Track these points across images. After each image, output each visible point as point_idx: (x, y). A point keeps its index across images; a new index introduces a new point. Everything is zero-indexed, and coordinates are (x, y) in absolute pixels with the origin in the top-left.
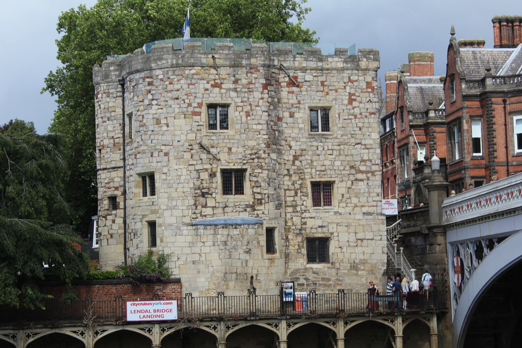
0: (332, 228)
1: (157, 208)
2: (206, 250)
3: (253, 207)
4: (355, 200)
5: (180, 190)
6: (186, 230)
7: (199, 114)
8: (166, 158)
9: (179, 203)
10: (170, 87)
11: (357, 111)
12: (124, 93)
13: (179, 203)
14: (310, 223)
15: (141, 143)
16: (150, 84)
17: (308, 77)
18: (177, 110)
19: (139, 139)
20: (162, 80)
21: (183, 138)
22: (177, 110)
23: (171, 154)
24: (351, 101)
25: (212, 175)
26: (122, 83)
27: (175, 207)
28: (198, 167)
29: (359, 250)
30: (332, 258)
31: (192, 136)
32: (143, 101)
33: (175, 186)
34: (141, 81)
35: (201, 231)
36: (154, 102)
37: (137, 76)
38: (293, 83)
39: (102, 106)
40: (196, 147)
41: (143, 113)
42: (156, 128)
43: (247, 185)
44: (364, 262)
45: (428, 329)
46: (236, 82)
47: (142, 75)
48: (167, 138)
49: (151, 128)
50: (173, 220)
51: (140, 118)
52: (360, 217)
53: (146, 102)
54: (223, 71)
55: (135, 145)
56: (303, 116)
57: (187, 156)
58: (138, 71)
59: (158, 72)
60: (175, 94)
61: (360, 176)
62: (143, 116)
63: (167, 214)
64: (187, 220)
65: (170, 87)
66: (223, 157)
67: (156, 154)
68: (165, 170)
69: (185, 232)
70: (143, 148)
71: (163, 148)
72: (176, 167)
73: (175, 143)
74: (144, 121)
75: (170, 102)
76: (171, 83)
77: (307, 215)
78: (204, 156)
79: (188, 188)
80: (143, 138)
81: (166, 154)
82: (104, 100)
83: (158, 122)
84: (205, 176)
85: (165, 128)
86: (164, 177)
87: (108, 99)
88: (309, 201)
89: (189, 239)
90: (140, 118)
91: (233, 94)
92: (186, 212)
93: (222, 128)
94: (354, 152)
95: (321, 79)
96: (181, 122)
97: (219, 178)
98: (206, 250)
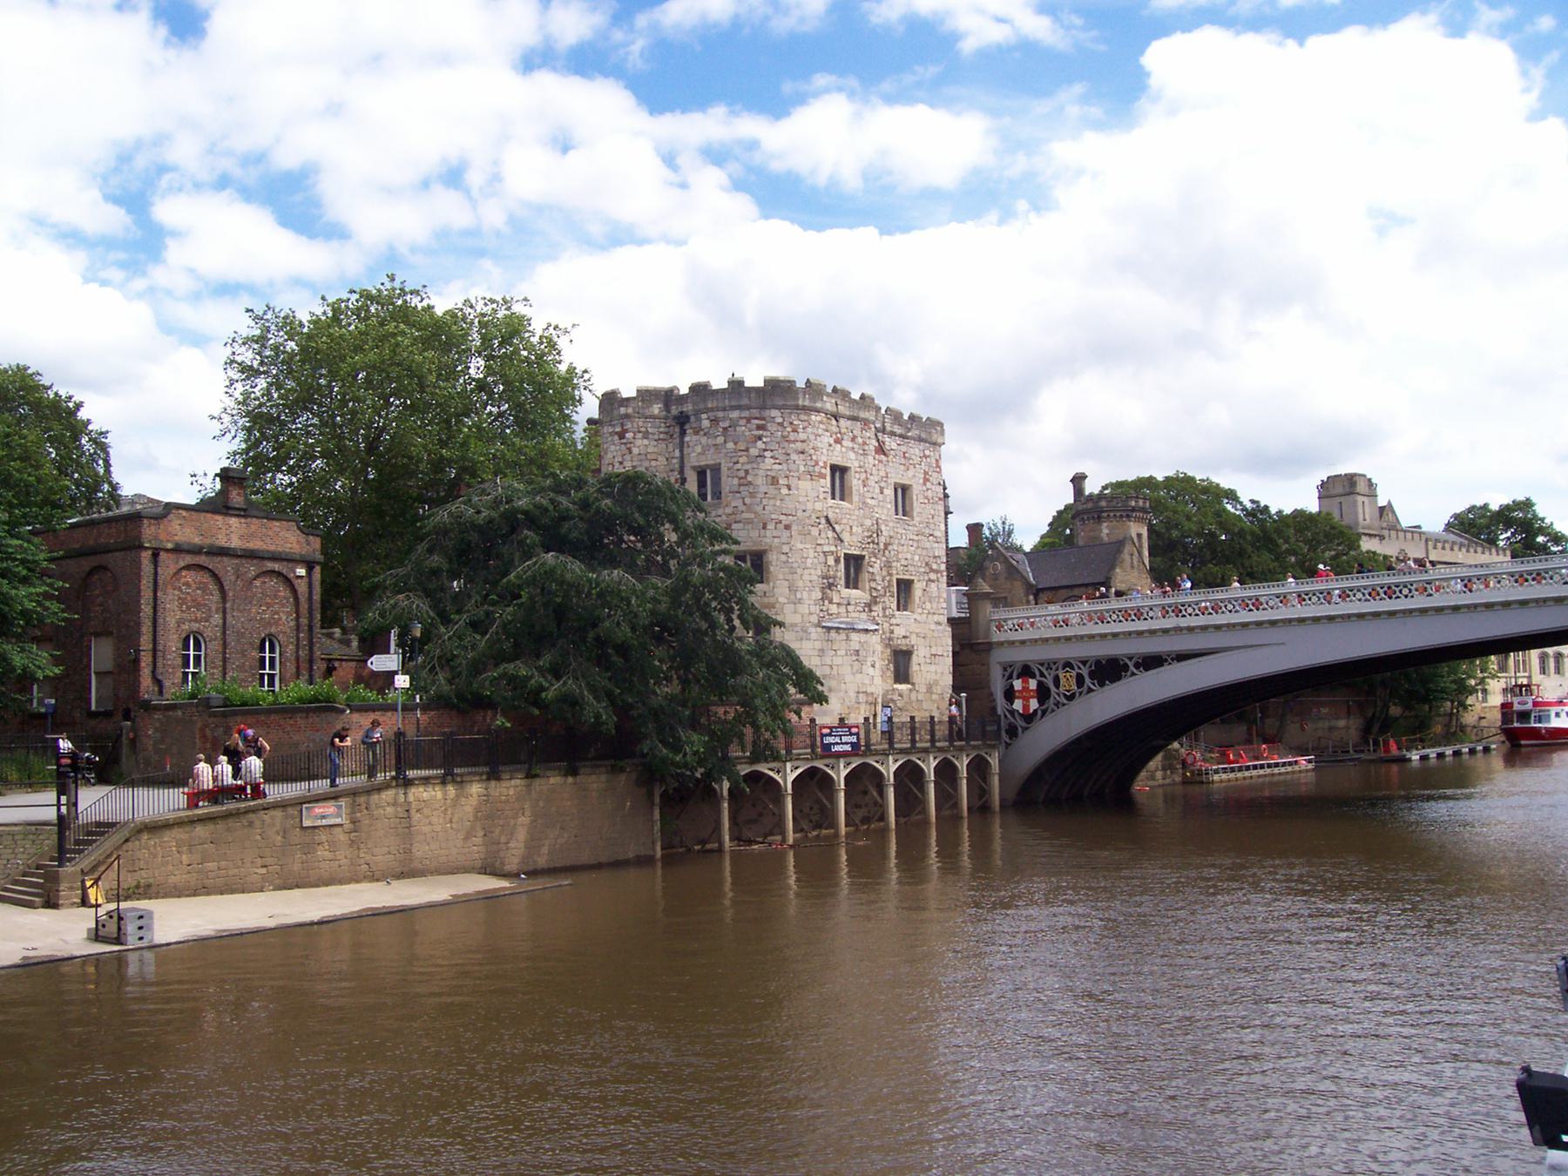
0: (914, 640)
1: (772, 600)
2: (838, 660)
3: (869, 606)
4: (928, 605)
5: (806, 577)
6: (815, 633)
7: (823, 476)
8: (786, 533)
9: (805, 595)
10: (792, 436)
11: (929, 494)
12: (683, 433)
13: (805, 595)
14: (899, 632)
15: (742, 508)
16: (759, 427)
17: (894, 446)
18: (802, 468)
19: (738, 503)
20: (780, 424)
21: (809, 506)
22: (802, 468)
23: (794, 527)
24: (926, 480)
25: (837, 561)
26: (682, 421)
27: (800, 601)
28: (826, 549)
29: (933, 668)
30: (916, 678)
31: (818, 506)
32: (747, 450)
33: (799, 571)
34: (743, 422)
35: (833, 634)
36: (768, 454)
37: (735, 414)
38: (881, 450)
39: (635, 451)
40: (823, 521)
41: (747, 467)
42: (772, 490)
43: (865, 576)
44: (936, 682)
45: (954, 769)
46: (853, 439)
47: (746, 414)
48: (789, 505)
49: (763, 489)
50: (797, 619)
51: (742, 474)
52: (933, 627)
53: (754, 452)
54: (842, 421)
55: (729, 510)
56: (889, 492)
57: (815, 531)
58: (739, 408)
59: (774, 413)
60: (799, 446)
61: (933, 576)
62: (747, 472)
63: (789, 608)
64: (814, 619)
65: (792, 436)
66: (846, 536)
67: (771, 526)
68: (786, 549)
69: (814, 636)
70: (746, 515)
71: (782, 518)
72: (800, 546)
73: (800, 513)
74: (749, 478)
75: (794, 456)
76: (795, 431)
77: (893, 621)
78: (830, 534)
79: (813, 575)
80: (747, 501)
81: (787, 527)
82: (639, 442)
83: (774, 481)
84: (831, 561)
85: (784, 491)
86: (783, 558)
87: (646, 442)
88: (894, 606)
89: (818, 645)
90: (742, 474)
91: (852, 455)
92: (813, 609)
93: (842, 499)
94: (928, 545)
95: (903, 449)
96: (805, 485)
97: (842, 565)
98: (838, 660)
